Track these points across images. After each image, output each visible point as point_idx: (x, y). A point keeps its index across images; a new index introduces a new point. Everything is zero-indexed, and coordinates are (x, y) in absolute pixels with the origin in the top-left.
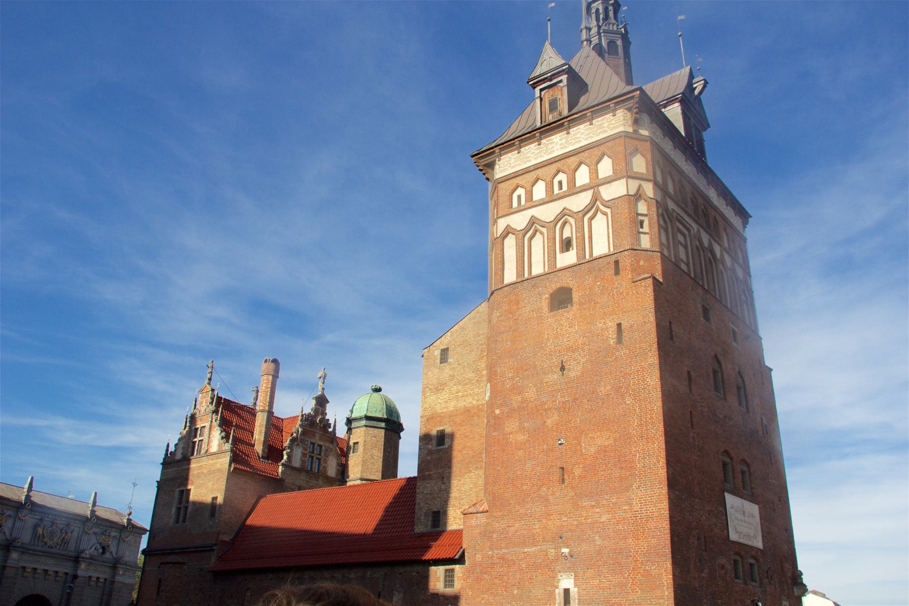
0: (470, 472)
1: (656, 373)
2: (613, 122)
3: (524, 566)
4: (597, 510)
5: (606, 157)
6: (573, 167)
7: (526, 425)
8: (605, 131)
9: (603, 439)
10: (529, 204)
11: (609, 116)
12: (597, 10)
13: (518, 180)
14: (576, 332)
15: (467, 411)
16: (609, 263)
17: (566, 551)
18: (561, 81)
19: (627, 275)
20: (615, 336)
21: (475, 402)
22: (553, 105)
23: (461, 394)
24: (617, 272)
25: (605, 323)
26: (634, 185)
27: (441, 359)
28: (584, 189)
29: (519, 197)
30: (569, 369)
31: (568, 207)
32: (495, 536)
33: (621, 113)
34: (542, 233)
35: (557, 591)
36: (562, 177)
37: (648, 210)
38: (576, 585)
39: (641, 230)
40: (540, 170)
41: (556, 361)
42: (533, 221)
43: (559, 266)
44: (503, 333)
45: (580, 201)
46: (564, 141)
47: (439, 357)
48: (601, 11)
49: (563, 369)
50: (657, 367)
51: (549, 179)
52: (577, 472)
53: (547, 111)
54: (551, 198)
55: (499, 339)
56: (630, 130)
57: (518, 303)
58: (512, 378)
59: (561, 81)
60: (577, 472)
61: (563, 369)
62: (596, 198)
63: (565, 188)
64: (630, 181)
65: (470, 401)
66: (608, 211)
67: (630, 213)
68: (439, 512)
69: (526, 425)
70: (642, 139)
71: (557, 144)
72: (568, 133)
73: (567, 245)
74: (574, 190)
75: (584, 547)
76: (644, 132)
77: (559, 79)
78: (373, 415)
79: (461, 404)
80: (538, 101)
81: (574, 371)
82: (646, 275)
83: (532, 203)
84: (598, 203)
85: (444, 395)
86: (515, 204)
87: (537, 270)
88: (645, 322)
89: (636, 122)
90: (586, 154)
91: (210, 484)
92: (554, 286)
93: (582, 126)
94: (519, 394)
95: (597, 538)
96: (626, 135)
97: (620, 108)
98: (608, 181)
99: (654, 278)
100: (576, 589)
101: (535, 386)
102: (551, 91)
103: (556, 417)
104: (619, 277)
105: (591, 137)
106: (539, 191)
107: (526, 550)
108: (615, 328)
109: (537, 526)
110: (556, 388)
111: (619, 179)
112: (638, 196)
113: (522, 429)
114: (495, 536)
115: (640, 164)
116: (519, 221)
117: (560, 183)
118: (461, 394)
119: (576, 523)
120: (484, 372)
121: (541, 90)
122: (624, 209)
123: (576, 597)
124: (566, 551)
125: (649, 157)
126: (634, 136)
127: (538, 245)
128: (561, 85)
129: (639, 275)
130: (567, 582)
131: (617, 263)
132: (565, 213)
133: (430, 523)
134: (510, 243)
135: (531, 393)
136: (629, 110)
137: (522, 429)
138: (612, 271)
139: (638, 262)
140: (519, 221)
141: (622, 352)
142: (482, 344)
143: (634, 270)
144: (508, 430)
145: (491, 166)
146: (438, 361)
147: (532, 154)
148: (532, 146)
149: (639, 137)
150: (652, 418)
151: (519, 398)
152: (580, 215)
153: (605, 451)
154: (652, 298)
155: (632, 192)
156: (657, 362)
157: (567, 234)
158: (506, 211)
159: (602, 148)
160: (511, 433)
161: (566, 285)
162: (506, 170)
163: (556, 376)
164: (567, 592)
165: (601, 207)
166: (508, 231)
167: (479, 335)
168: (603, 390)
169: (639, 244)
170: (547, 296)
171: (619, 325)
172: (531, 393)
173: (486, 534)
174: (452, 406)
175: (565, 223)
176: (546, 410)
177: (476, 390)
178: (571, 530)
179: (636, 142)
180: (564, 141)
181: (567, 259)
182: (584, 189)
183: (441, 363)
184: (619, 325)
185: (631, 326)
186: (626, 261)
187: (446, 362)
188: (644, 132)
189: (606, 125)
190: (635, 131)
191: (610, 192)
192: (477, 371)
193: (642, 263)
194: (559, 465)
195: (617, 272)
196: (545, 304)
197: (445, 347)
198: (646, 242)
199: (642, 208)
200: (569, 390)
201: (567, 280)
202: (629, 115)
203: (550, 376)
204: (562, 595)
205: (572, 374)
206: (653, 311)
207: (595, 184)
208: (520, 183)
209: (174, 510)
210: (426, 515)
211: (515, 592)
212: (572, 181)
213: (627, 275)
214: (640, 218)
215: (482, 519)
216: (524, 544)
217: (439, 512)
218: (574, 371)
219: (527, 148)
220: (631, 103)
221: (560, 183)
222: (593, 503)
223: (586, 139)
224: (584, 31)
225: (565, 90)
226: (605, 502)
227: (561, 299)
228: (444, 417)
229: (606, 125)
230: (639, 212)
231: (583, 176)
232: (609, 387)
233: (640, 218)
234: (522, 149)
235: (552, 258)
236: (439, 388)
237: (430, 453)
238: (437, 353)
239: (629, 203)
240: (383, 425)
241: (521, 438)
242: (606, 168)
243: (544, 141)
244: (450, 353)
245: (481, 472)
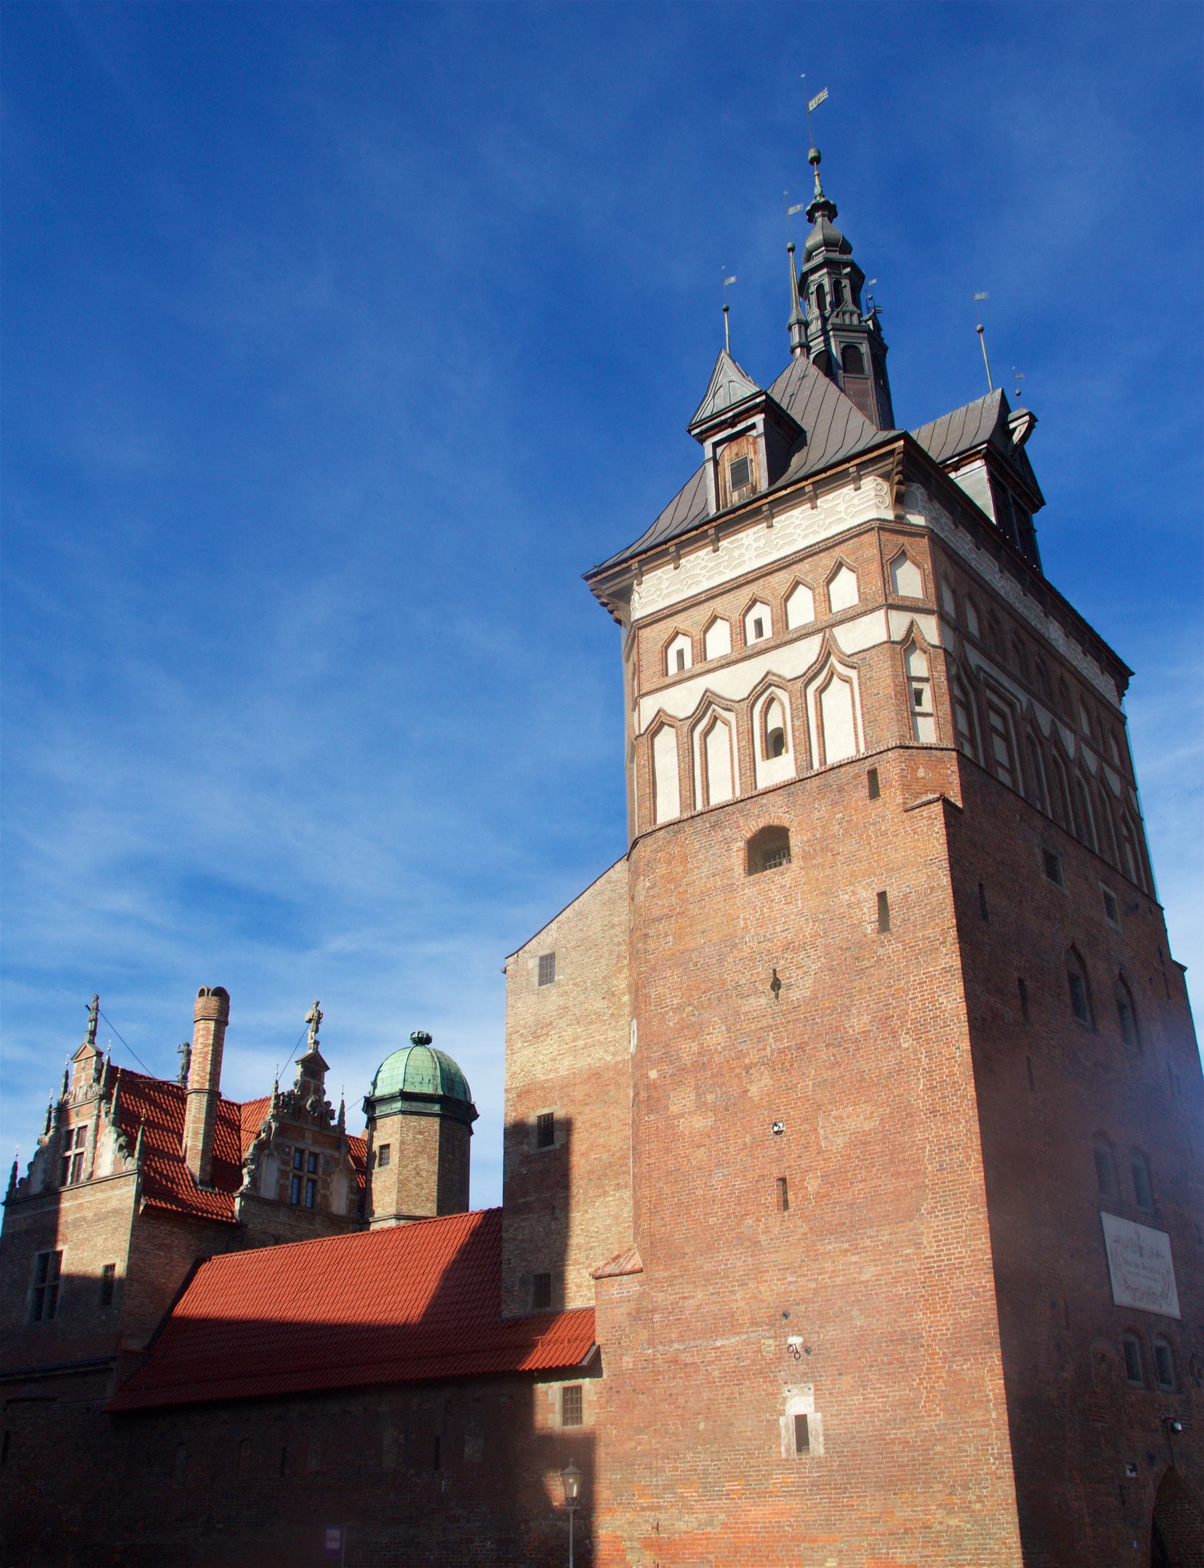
0: (605, 1194)
1: (958, 988)
2: (856, 501)
3: (716, 1373)
4: (855, 1258)
5: (844, 568)
6: (782, 591)
7: (710, 1098)
8: (840, 520)
9: (859, 1119)
10: (699, 667)
11: (848, 490)
12: (820, 287)
13: (678, 622)
14: (800, 913)
15: (595, 1075)
16: (857, 776)
17: (796, 1340)
18: (753, 426)
19: (893, 796)
20: (875, 917)
21: (609, 1058)
22: (741, 471)
23: (581, 1043)
24: (874, 793)
25: (854, 893)
26: (900, 622)
27: (541, 976)
28: (805, 634)
29: (680, 654)
30: (789, 986)
31: (774, 671)
32: (657, 1317)
33: (870, 483)
34: (726, 723)
35: (782, 1420)
36: (760, 611)
37: (931, 669)
38: (818, 1408)
39: (918, 709)
40: (718, 600)
41: (763, 973)
42: (708, 701)
43: (762, 785)
44: (659, 920)
45: (796, 659)
46: (762, 542)
47: (536, 972)
48: (827, 288)
49: (776, 985)
50: (958, 974)
51: (736, 617)
52: (813, 1185)
53: (729, 484)
55: (652, 932)
56: (890, 515)
57: (684, 860)
58: (678, 1009)
59: (753, 426)
60: (813, 1185)
61: (776, 985)
63: (768, 631)
64: (893, 614)
65: (601, 1056)
66: (853, 674)
67: (895, 677)
68: (549, 1275)
69: (710, 1098)
70: (913, 532)
71: (750, 548)
72: (770, 526)
73: (775, 743)
74: (786, 638)
75: (831, 1332)
76: (917, 520)
77: (750, 422)
78: (417, 1089)
79: (583, 1062)
80: (710, 466)
82: (931, 797)
83: (704, 665)
84: (832, 658)
85: (549, 1047)
86: (673, 668)
87: (721, 794)
88: (932, 888)
89: (900, 500)
90: (806, 565)
91: (99, 1241)
92: (753, 826)
93: (796, 512)
94: (693, 1039)
95: (855, 1312)
96: (881, 526)
97: (869, 474)
98: (850, 616)
99: (946, 802)
100: (819, 1415)
101: (724, 1020)
102: (734, 447)
103: (766, 1080)
104: (879, 802)
105: (815, 532)
106: (719, 641)
107: (718, 1344)
108: (874, 902)
109: (738, 1296)
110: (764, 1023)
111: (872, 611)
112: (909, 643)
113: (701, 1106)
114: (657, 1317)
115: (911, 581)
116: (681, 701)
117: (759, 624)
118: (581, 1043)
119: (813, 1285)
120: (626, 998)
121: (716, 445)
122: (883, 672)
123: (821, 1430)
124: (796, 1340)
125: (928, 566)
126: (898, 527)
127: (721, 747)
128: (754, 433)
129: (917, 795)
130: (800, 1402)
131: (873, 774)
132: (767, 683)
133: (530, 1298)
134: (666, 742)
135: (716, 1037)
136: (886, 476)
137: (701, 1106)
138: (866, 791)
139: (916, 770)
141: (891, 948)
142: (619, 944)
143: (906, 788)
144: (674, 1109)
145: (625, 595)
146: (536, 980)
147: (702, 569)
148: (702, 553)
149: (907, 528)
150: (952, 1074)
151: (695, 1047)
152: (799, 684)
153: (866, 1143)
154: (943, 840)
155: (898, 636)
156: (958, 963)
157: (774, 722)
158: (657, 682)
159: (837, 553)
160: (682, 1115)
161: (776, 822)
162: (653, 601)
163: (763, 1001)
164: (801, 1421)
165: (840, 668)
166: (660, 723)
167: (613, 926)
168: (858, 1022)
169: (916, 738)
170: (741, 844)
171: (882, 896)
172: (716, 1037)
173: (640, 1314)
174: (564, 1067)
175: (771, 701)
176: (747, 1069)
177: (610, 1034)
178: (804, 1301)
179: (902, 539)
180: (762, 542)
181: (779, 770)
182: (805, 634)
183: (541, 983)
184: (882, 896)
185: (906, 896)
186: (891, 769)
187: (551, 980)
188: (917, 520)
189: (842, 507)
190: (899, 518)
191: (851, 638)
192: (610, 995)
193: (921, 773)
194: (777, 1173)
195: (874, 793)
196: (737, 858)
197: (547, 952)
198: (927, 732)
199: (919, 665)
200: (791, 1026)
201: (776, 813)
202: (886, 486)
203: (752, 1000)
204: (792, 1427)
205: (795, 995)
206: (946, 864)
207: (825, 626)
208: (682, 627)
209: (30, 1295)
210: (523, 1282)
211: (702, 1426)
212: (782, 619)
213: (893, 796)
214: (915, 685)
215: (631, 1286)
216: (715, 1332)
217: (549, 1275)
218: (799, 990)
219: (692, 557)
220: (888, 465)
221: (759, 624)
222: (846, 1246)
223: (804, 537)
224: (796, 329)
225: (762, 442)
226: (868, 1242)
227: (768, 849)
228: (551, 1089)
229: (842, 507)
230: (913, 674)
231: (802, 608)
232: (866, 1018)
233: (915, 685)
234: (683, 561)
235: (749, 770)
236: (537, 1035)
237: (526, 1159)
238: (533, 964)
239: (893, 658)
240: (436, 1108)
241: (700, 1123)
243: (724, 544)
244: (559, 963)
245: (627, 1194)
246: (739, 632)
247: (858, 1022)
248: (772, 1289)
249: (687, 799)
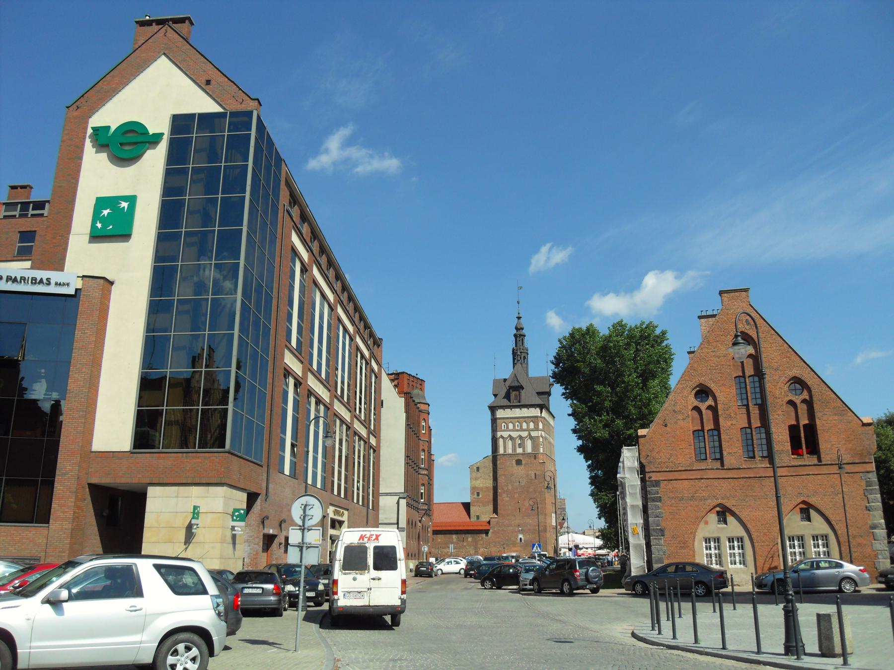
54: (514, 430)
62: (530, 434)
71: (517, 413)
74: (522, 430)
81: (523, 484)
83: (507, 430)
85: (478, 482)
87: (510, 451)
127: (510, 443)
135: (510, 487)
140: (505, 434)
173: (498, 523)
174: (481, 485)
181: (519, 451)
182: (525, 430)
196: (514, 462)
212: (521, 426)
227: (519, 462)
231: (525, 426)
236: (476, 479)
242: (532, 425)
246: (514, 426)
247: (531, 490)
248: (517, 522)
249: (505, 451)
